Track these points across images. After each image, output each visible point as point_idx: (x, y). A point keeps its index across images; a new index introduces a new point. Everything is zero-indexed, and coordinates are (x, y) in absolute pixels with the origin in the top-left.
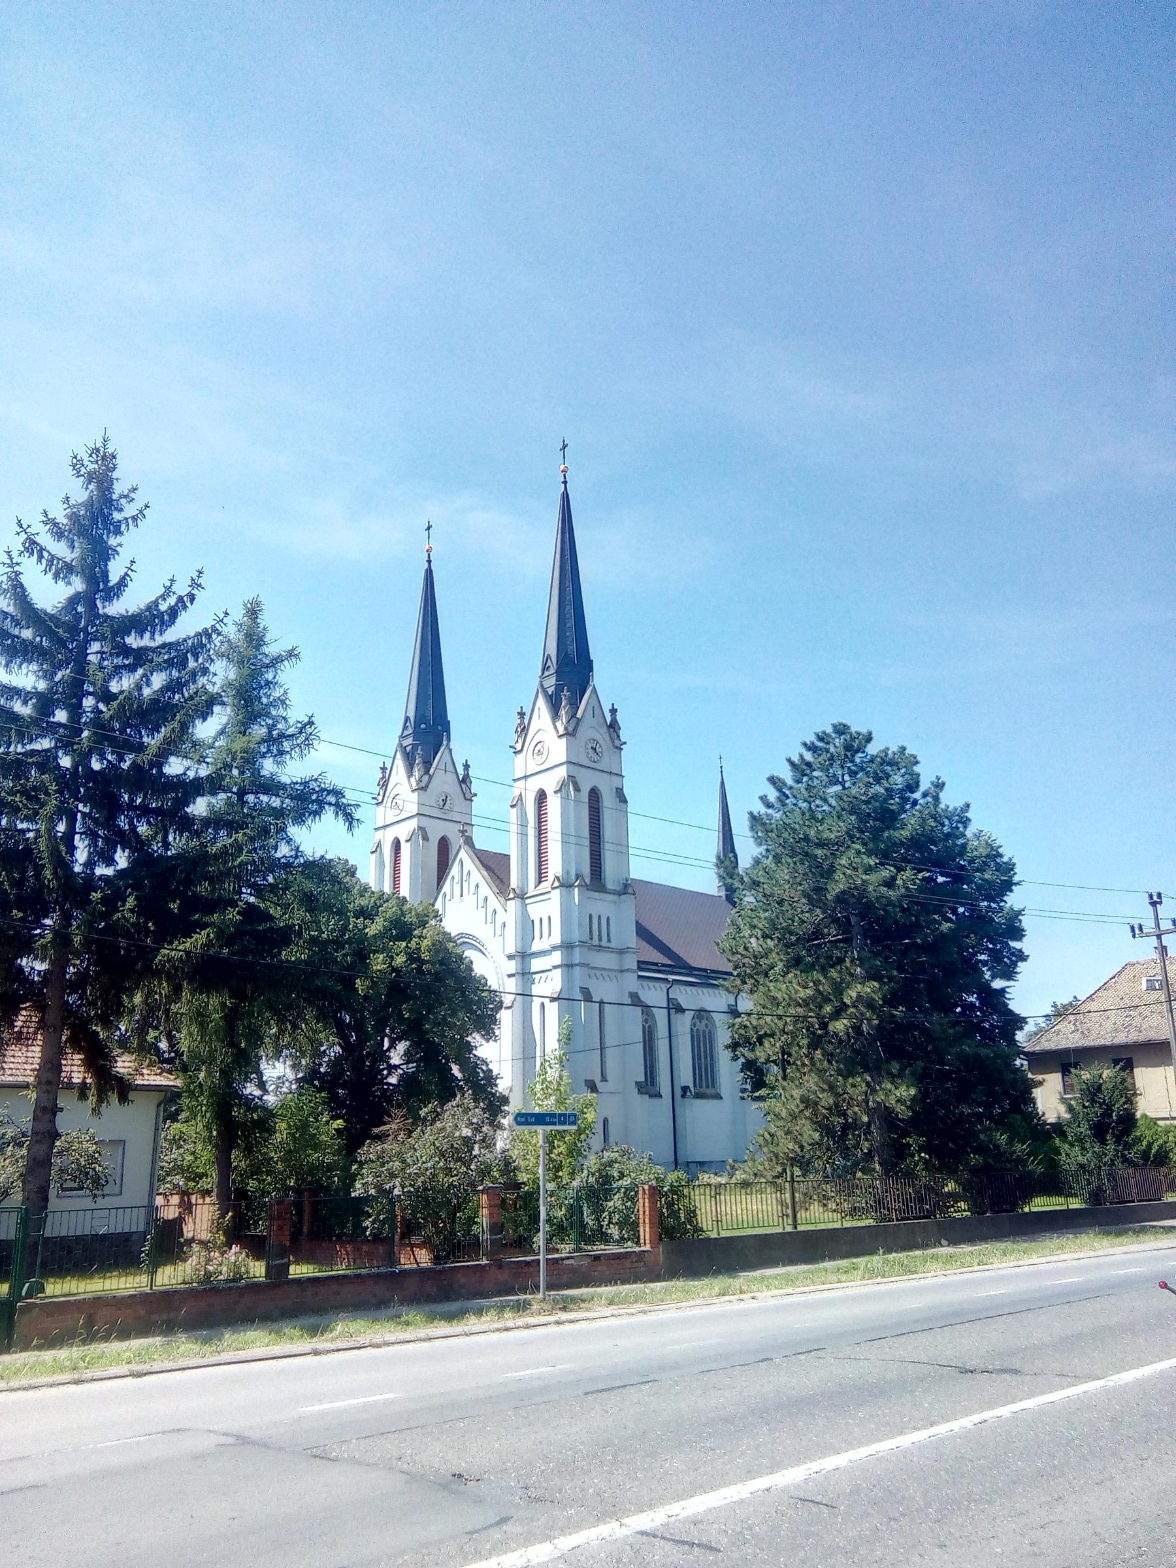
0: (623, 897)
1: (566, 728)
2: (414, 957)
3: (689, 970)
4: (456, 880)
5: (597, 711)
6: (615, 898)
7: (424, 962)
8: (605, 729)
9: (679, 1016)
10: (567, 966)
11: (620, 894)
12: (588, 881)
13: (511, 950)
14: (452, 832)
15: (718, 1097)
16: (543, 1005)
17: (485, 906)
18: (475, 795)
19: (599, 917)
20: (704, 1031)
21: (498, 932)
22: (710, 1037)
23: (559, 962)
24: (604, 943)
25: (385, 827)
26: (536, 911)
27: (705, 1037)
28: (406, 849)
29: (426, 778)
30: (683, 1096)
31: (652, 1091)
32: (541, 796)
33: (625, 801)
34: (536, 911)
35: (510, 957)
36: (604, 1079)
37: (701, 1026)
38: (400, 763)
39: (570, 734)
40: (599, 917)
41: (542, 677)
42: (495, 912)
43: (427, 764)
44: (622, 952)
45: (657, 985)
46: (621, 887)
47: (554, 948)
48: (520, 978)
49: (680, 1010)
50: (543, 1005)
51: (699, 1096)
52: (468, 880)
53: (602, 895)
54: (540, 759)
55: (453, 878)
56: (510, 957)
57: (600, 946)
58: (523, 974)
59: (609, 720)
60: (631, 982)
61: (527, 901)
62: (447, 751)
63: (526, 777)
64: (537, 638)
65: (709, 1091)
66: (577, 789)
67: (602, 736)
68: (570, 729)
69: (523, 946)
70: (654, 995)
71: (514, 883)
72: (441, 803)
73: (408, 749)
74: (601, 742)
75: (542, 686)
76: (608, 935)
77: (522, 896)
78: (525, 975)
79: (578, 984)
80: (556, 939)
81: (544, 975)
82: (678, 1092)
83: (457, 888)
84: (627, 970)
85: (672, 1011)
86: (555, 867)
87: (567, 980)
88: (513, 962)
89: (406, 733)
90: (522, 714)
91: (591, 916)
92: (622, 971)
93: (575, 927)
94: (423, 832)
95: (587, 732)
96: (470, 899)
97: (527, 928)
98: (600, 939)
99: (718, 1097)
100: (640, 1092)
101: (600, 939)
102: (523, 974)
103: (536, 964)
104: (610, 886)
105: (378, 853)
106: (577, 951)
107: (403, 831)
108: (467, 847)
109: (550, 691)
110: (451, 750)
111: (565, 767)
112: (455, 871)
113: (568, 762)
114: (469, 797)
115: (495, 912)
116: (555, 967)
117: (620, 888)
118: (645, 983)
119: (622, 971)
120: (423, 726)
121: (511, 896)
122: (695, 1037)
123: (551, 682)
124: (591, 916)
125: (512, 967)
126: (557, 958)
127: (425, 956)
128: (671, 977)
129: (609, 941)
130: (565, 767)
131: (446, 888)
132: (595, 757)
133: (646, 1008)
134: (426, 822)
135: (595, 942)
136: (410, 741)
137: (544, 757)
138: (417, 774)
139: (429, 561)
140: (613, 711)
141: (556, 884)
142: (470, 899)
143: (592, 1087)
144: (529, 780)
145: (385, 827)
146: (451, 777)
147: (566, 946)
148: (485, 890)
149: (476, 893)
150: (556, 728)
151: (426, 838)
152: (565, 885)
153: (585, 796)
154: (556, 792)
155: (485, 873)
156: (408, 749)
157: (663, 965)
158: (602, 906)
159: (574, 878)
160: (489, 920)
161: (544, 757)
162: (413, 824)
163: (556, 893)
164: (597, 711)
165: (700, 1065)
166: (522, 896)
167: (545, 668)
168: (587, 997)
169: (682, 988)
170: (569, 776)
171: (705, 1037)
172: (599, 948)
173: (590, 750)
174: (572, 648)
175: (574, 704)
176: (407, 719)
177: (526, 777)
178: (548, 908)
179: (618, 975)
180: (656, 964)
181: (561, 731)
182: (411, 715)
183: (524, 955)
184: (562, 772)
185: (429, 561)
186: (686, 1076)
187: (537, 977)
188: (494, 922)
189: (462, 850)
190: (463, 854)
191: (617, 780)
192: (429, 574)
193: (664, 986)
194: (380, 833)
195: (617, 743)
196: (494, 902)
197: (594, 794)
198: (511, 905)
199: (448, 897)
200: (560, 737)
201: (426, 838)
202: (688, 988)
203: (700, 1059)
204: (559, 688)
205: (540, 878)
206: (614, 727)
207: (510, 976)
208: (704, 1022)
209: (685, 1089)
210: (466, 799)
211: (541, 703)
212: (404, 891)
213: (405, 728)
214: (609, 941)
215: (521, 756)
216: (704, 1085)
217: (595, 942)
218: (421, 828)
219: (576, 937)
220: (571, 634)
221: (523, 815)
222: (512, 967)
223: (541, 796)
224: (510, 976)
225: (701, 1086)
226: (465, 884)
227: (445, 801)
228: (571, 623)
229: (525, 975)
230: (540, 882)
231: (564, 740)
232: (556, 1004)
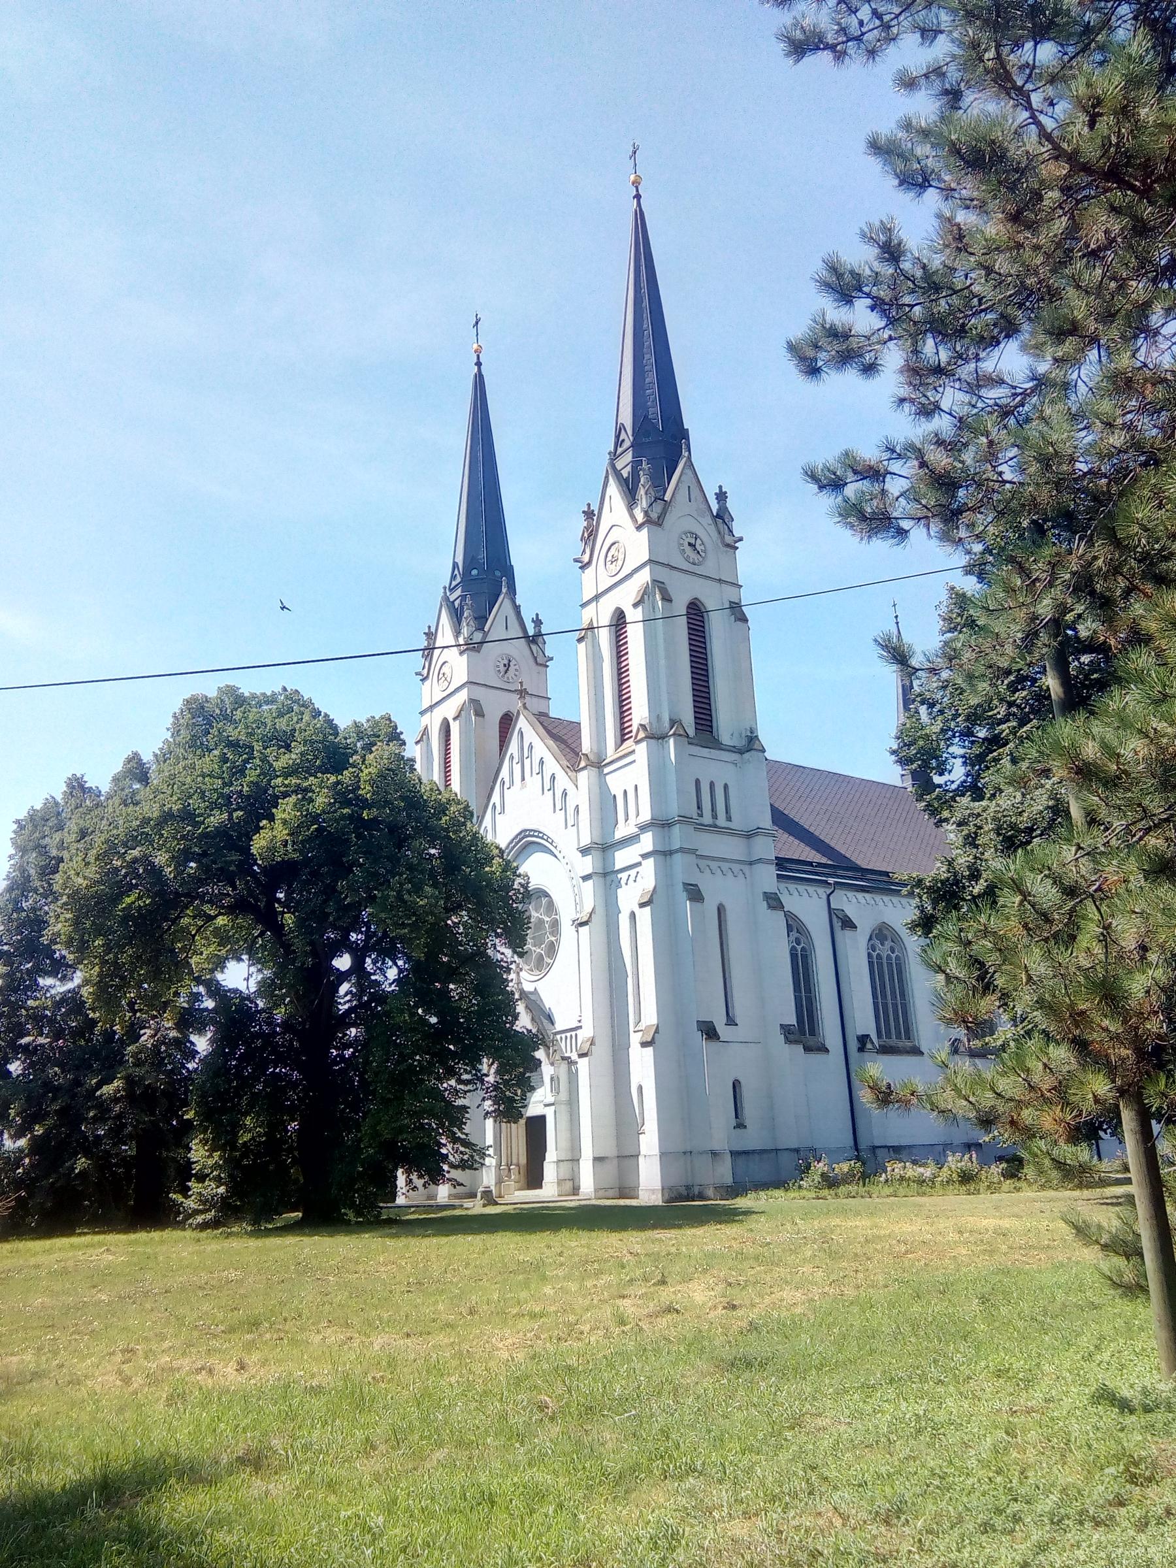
0: (747, 756)
1: (646, 513)
2: (345, 796)
3: (864, 872)
4: (516, 760)
5: (695, 492)
6: (734, 757)
7: (365, 804)
8: (709, 520)
9: (848, 933)
10: (662, 854)
11: (741, 752)
12: (691, 732)
13: (586, 840)
14: (514, 703)
15: (916, 1051)
16: (633, 915)
17: (552, 788)
18: (552, 659)
19: (712, 785)
20: (889, 957)
21: (571, 822)
22: (899, 966)
23: (650, 848)
24: (722, 821)
25: (431, 708)
26: (617, 782)
27: (890, 965)
28: (455, 727)
29: (478, 637)
30: (861, 1049)
31: (811, 1041)
32: (619, 621)
33: (746, 621)
34: (617, 782)
35: (584, 851)
36: (731, 1021)
37: (884, 950)
38: (445, 619)
39: (654, 522)
40: (712, 785)
41: (614, 456)
42: (565, 794)
43: (481, 620)
44: (749, 835)
45: (811, 889)
46: (744, 742)
47: (643, 828)
48: (601, 880)
49: (848, 924)
50: (633, 915)
51: (885, 1050)
52: (530, 756)
53: (715, 753)
54: (613, 568)
55: (512, 757)
56: (584, 851)
57: (716, 826)
58: (605, 875)
59: (715, 507)
60: (767, 877)
61: (606, 770)
62: (507, 604)
63: (597, 597)
64: (609, 403)
65: (904, 1043)
66: (667, 599)
67: (707, 532)
68: (654, 516)
69: (603, 836)
70: (808, 904)
71: (586, 746)
72: (503, 669)
73: (457, 603)
74: (701, 532)
75: (613, 467)
76: (727, 811)
77: (598, 764)
78: (607, 878)
79: (680, 877)
80: (646, 815)
81: (633, 872)
82: (853, 1045)
83: (517, 769)
84: (759, 861)
85: (837, 925)
86: (640, 712)
87: (664, 876)
88: (589, 859)
89: (454, 583)
90: (589, 514)
91: (698, 782)
92: (751, 863)
93: (673, 795)
94: (476, 707)
95: (681, 519)
96: (534, 782)
97: (606, 806)
98: (715, 817)
99: (916, 1051)
100: (788, 1041)
101: (715, 817)
102: (605, 875)
103: (622, 858)
104: (726, 739)
105: (423, 744)
106: (676, 829)
107: (449, 710)
108: (526, 712)
109: (625, 474)
110: (517, 609)
111: (647, 569)
112: (513, 748)
113: (650, 561)
114: (542, 663)
115: (565, 794)
116: (645, 856)
117: (740, 743)
118: (792, 886)
119: (751, 863)
120: (474, 572)
121: (583, 764)
122: (875, 966)
123: (625, 462)
124: (698, 782)
125: (587, 865)
126: (647, 842)
127: (366, 791)
128: (831, 880)
129: (729, 819)
130: (647, 569)
131: (504, 773)
132: (693, 556)
133: (794, 926)
134: (480, 694)
135: (707, 819)
136: (458, 592)
137: (620, 563)
138: (465, 631)
139: (479, 364)
140: (721, 496)
141: (642, 735)
142: (534, 782)
143: (710, 1032)
144: (602, 600)
145: (431, 708)
146: (515, 631)
147: (660, 824)
148: (552, 766)
149: (541, 772)
150: (633, 517)
151: (479, 713)
152: (655, 736)
153: (680, 606)
154: (635, 605)
155: (551, 742)
156: (457, 603)
157: (820, 865)
158: (715, 768)
159: (667, 724)
160: (558, 806)
161: (620, 563)
162: (463, 696)
163: (642, 750)
164: (695, 492)
165: (885, 1006)
166: (598, 764)
167: (618, 442)
168: (695, 894)
169: (850, 894)
170: (654, 581)
171: (890, 965)
172: (714, 828)
173: (689, 550)
174: (655, 411)
175: (659, 485)
176: (455, 565)
177: (597, 597)
178: (632, 776)
179: (746, 868)
180: (810, 864)
181: (640, 517)
182: (460, 560)
183: (604, 847)
184: (645, 576)
185: (479, 364)
186: (864, 1020)
187: (623, 876)
188: (564, 808)
189: (522, 717)
190: (522, 723)
191: (729, 593)
192: (479, 383)
193: (822, 892)
194: (425, 720)
195: (728, 539)
196: (563, 781)
197: (696, 614)
198: (583, 777)
199: (507, 785)
200: (639, 528)
201: (479, 713)
202: (860, 895)
203: (884, 996)
204: (636, 465)
205: (623, 735)
206: (722, 517)
207: (585, 878)
208: (888, 944)
209: (863, 1040)
210: (537, 663)
211: (613, 490)
212: (456, 786)
213: (453, 577)
214: (729, 819)
215: (590, 571)
216: (894, 1033)
217: (707, 819)
218: (473, 701)
219: (673, 811)
220: (653, 392)
221: (596, 646)
222: (587, 865)
223: (619, 621)
224: (585, 878)
225: (889, 1036)
226: (527, 762)
227: (507, 666)
228: (652, 377)
229: (607, 877)
230: (623, 741)
231: (645, 531)
232: (648, 909)
